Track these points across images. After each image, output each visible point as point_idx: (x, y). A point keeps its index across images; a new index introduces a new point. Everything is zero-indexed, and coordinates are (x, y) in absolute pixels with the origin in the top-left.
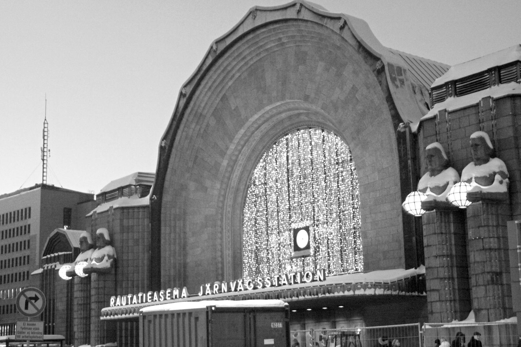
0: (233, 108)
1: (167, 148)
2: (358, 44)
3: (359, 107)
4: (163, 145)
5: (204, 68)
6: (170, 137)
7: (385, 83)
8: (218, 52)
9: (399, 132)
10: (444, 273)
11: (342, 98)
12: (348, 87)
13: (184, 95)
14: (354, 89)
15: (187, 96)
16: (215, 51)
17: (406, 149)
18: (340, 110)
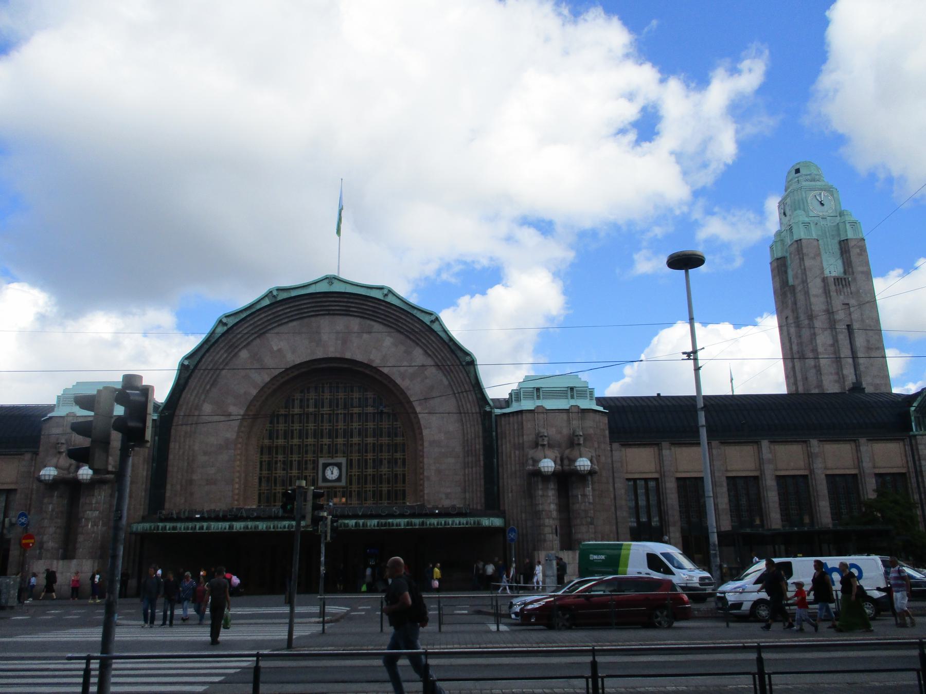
0: (275, 348)
1: (192, 367)
4: (186, 363)
5: (258, 307)
6: (197, 358)
8: (279, 298)
10: (555, 514)
13: (225, 324)
15: (229, 326)
16: (274, 296)
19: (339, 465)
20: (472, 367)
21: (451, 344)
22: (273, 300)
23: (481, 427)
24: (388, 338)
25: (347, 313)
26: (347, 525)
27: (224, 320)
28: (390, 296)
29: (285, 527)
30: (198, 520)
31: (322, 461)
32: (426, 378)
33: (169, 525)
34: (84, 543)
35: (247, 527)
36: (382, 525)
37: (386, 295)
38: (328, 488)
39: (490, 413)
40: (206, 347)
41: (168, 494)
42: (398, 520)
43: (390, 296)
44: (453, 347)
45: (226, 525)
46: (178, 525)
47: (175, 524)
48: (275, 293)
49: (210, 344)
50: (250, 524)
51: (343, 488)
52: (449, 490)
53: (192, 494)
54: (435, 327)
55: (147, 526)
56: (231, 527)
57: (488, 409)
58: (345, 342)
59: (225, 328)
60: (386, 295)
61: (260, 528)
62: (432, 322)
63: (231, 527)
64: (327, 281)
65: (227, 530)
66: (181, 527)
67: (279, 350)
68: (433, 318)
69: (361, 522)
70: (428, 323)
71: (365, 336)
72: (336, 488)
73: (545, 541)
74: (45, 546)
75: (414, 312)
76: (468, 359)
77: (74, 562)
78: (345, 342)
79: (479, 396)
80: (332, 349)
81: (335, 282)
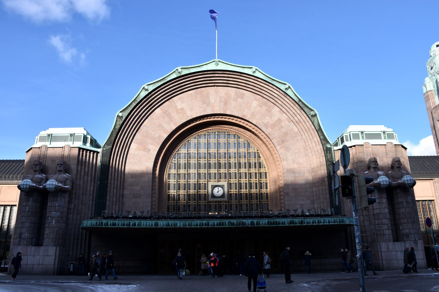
0: (179, 108)
1: (124, 118)
2: (298, 100)
3: (283, 130)
4: (120, 114)
5: (169, 79)
7: (317, 122)
8: (183, 74)
9: (326, 147)
11: (271, 122)
12: (275, 119)
13: (147, 90)
14: (279, 120)
15: (150, 91)
16: (179, 73)
17: (332, 156)
18: (269, 128)
19: (222, 187)
20: (315, 118)
21: (300, 103)
22: (179, 75)
23: (324, 158)
24: (255, 101)
25: (227, 85)
26: (244, 224)
27: (146, 87)
28: (257, 72)
29: (197, 225)
30: (130, 218)
31: (210, 184)
32: (282, 127)
33: (110, 222)
34: (49, 233)
35: (169, 225)
36: (271, 224)
37: (254, 72)
38: (215, 202)
39: (331, 148)
40: (134, 104)
41: (107, 203)
42: (283, 220)
43: (257, 72)
44: (301, 105)
45: (153, 222)
46: (117, 222)
47: (115, 222)
48: (180, 70)
49: (136, 102)
50: (171, 222)
51: (226, 202)
52: (302, 203)
53: (123, 204)
54: (289, 92)
55: (94, 222)
56: (156, 224)
57: (328, 146)
58: (226, 104)
59: (147, 93)
60: (254, 72)
61: (178, 225)
62: (286, 89)
63: (156, 224)
64: (214, 63)
65: (153, 227)
66: (119, 223)
67: (182, 109)
68: (287, 86)
69: (255, 221)
70: (284, 90)
71: (239, 100)
72: (221, 202)
73: (384, 235)
74: (23, 236)
75: (274, 83)
76: (312, 113)
77: (42, 248)
78: (226, 104)
79: (322, 137)
80: (217, 108)
81: (220, 63)
